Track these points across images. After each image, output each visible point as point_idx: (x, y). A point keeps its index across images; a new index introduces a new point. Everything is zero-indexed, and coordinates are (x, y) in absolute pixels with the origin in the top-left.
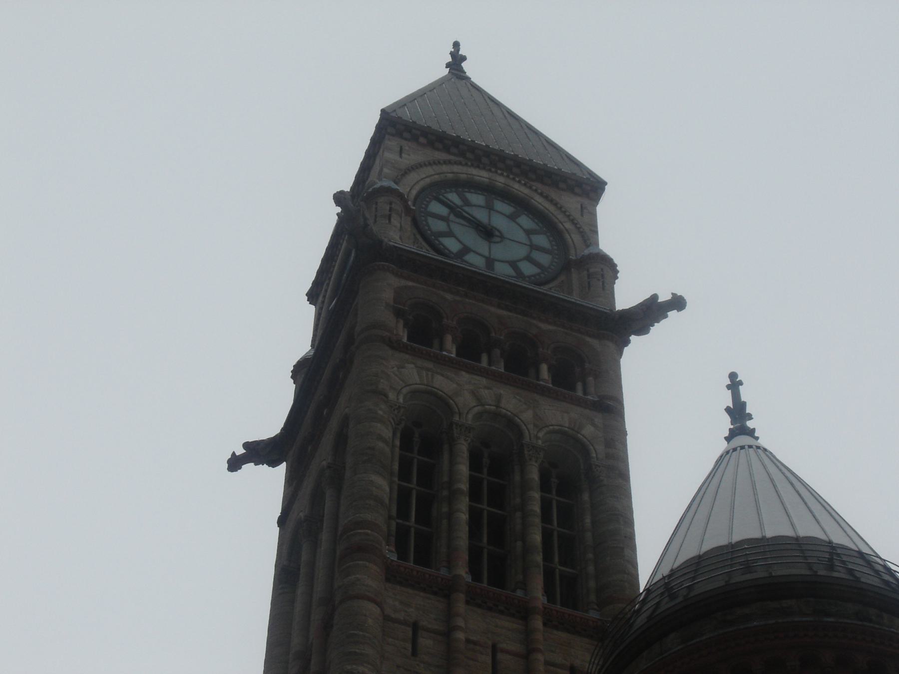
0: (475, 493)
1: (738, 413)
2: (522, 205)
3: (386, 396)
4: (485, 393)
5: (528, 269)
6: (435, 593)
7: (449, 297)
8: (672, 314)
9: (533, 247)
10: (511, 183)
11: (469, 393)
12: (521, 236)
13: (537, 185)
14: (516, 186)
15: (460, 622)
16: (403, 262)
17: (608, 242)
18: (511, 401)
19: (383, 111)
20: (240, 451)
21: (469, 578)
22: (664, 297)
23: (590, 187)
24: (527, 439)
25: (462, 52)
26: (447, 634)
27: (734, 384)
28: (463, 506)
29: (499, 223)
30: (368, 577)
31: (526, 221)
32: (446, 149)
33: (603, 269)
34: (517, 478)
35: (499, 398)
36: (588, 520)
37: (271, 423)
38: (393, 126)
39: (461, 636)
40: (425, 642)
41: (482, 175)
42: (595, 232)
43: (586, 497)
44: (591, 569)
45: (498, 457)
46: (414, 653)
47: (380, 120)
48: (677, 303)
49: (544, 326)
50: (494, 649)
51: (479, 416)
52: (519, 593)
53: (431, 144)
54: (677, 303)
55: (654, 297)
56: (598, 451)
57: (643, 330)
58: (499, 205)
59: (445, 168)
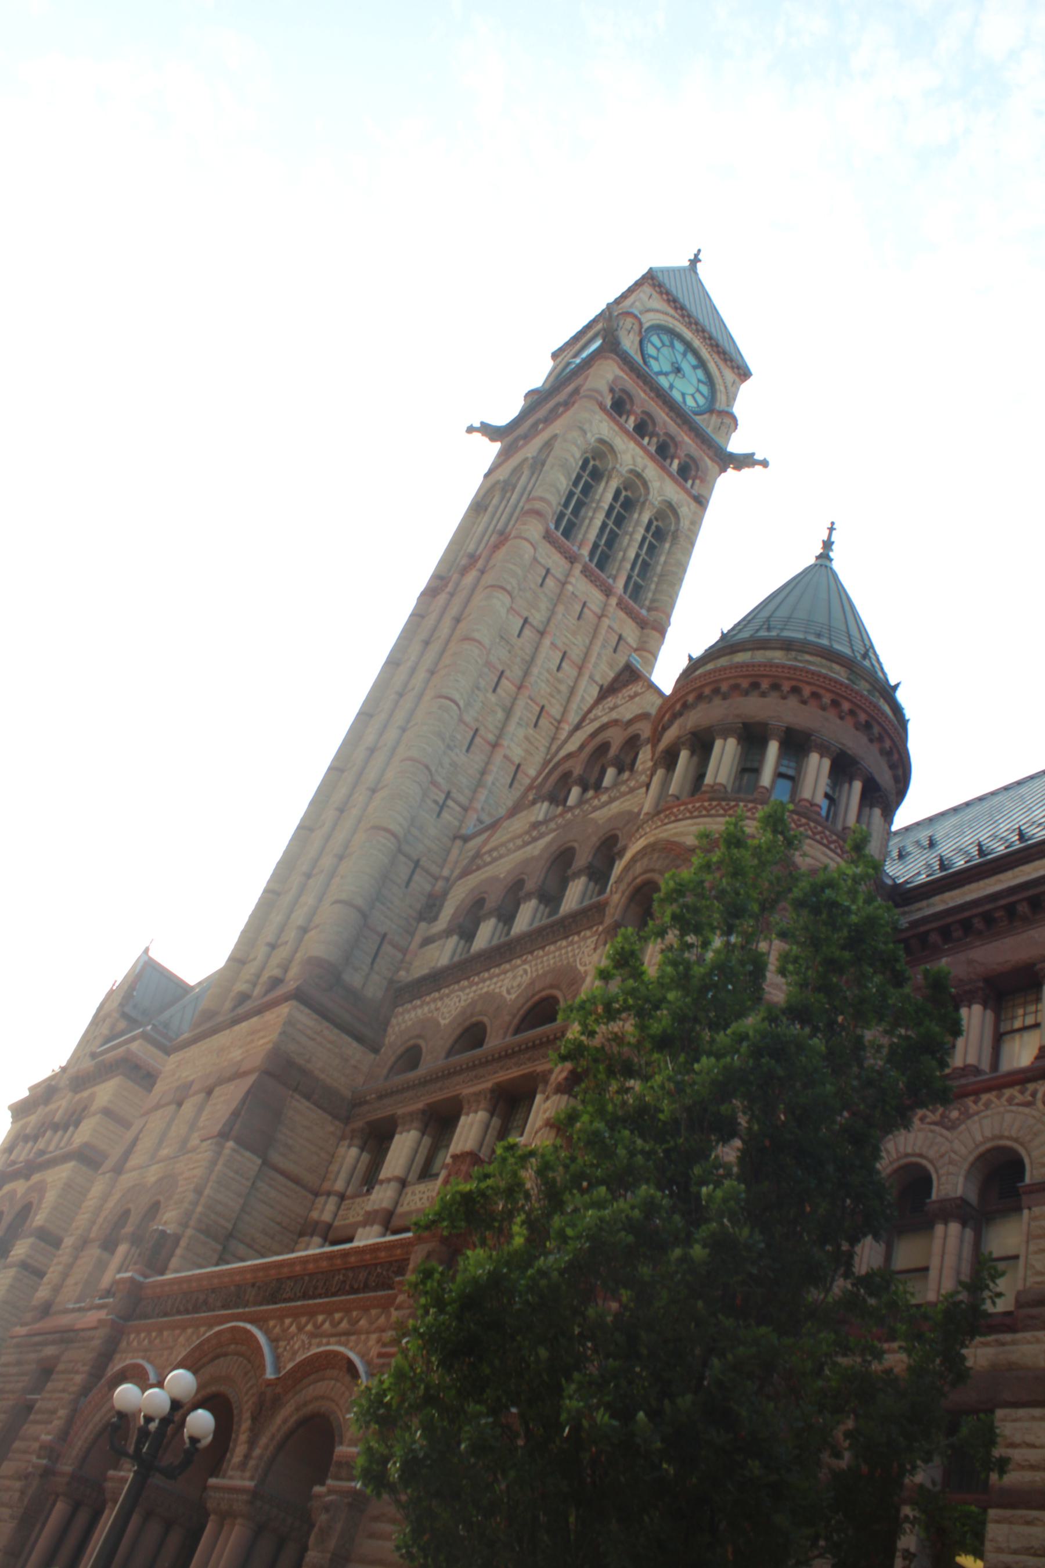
1: (828, 545)
2: (702, 364)
3: (585, 433)
4: (639, 460)
5: (690, 402)
6: (566, 558)
7: (642, 395)
8: (758, 468)
9: (698, 390)
10: (702, 347)
11: (631, 455)
12: (695, 381)
13: (715, 356)
15: (573, 580)
16: (626, 360)
17: (738, 409)
18: (651, 471)
19: (651, 268)
20: (477, 425)
21: (587, 559)
22: (758, 457)
23: (743, 373)
24: (650, 497)
25: (700, 257)
26: (564, 584)
27: (831, 529)
28: (600, 517)
29: (686, 367)
30: (534, 529)
31: (700, 373)
32: (676, 308)
33: (730, 422)
34: (636, 516)
35: (645, 467)
36: (662, 559)
37: (502, 417)
38: (651, 279)
40: (550, 582)
41: (688, 335)
42: (735, 400)
43: (667, 546)
44: (653, 586)
46: (542, 585)
47: (647, 273)
48: (764, 464)
49: (687, 439)
50: (584, 604)
51: (631, 471)
52: (610, 581)
53: (668, 301)
54: (764, 464)
55: (753, 454)
56: (685, 523)
57: (738, 468)
58: (690, 357)
59: (670, 319)
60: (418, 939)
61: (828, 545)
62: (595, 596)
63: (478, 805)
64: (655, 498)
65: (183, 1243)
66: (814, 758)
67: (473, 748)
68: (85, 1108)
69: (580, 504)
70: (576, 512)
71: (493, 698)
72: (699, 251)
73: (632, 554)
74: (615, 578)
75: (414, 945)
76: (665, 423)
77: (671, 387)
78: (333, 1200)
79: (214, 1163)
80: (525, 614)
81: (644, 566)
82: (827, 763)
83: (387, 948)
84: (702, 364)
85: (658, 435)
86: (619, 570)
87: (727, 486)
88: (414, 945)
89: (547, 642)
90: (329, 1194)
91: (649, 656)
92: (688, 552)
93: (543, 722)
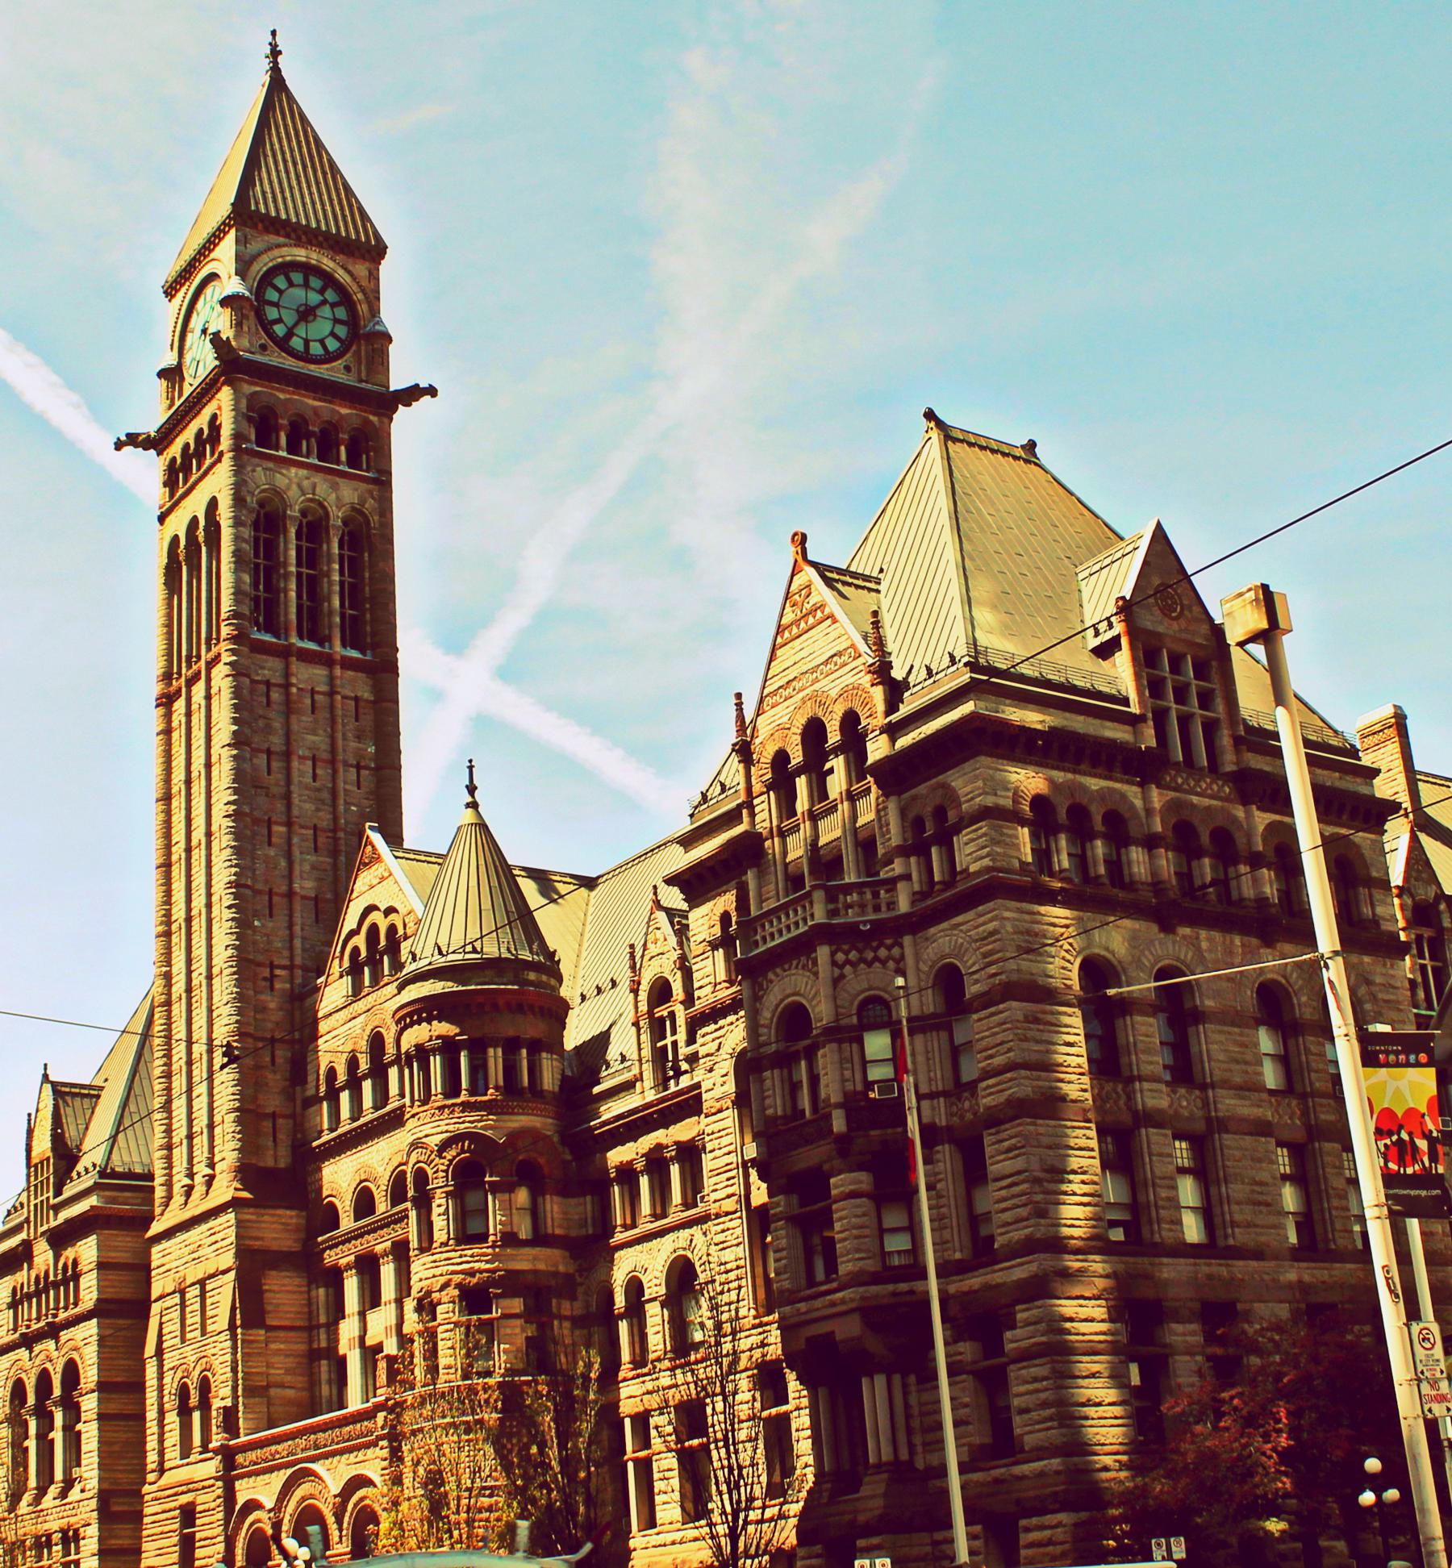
0: (299, 564)
1: (472, 789)
4: (306, 483)
7: (282, 396)
9: (336, 321)
11: (297, 483)
14: (325, 260)
15: (294, 680)
18: (322, 488)
23: (375, 251)
26: (287, 686)
27: (471, 768)
34: (325, 547)
36: (367, 575)
39: (294, 690)
40: (275, 695)
41: (300, 254)
45: (314, 528)
48: (432, 391)
49: (344, 411)
54: (432, 391)
56: (375, 519)
57: (409, 405)
59: (276, 252)
60: (299, 1103)
61: (472, 789)
62: (320, 672)
63: (298, 961)
64: (337, 516)
65: (241, 1408)
66: (491, 1051)
67: (275, 911)
68: (75, 1263)
69: (269, 572)
70: (269, 587)
71: (272, 852)
72: (274, 33)
73: (336, 603)
74: (329, 639)
75: (298, 1110)
76: (315, 410)
77: (307, 342)
78: (322, 1330)
79: (234, 1348)
80: (266, 746)
81: (352, 593)
82: (500, 1051)
83: (280, 1121)
84: (329, 280)
85: (313, 434)
86: (330, 627)
87: (407, 429)
88: (298, 1110)
89: (295, 764)
90: (319, 1326)
91: (389, 705)
92: (389, 555)
93: (321, 840)
